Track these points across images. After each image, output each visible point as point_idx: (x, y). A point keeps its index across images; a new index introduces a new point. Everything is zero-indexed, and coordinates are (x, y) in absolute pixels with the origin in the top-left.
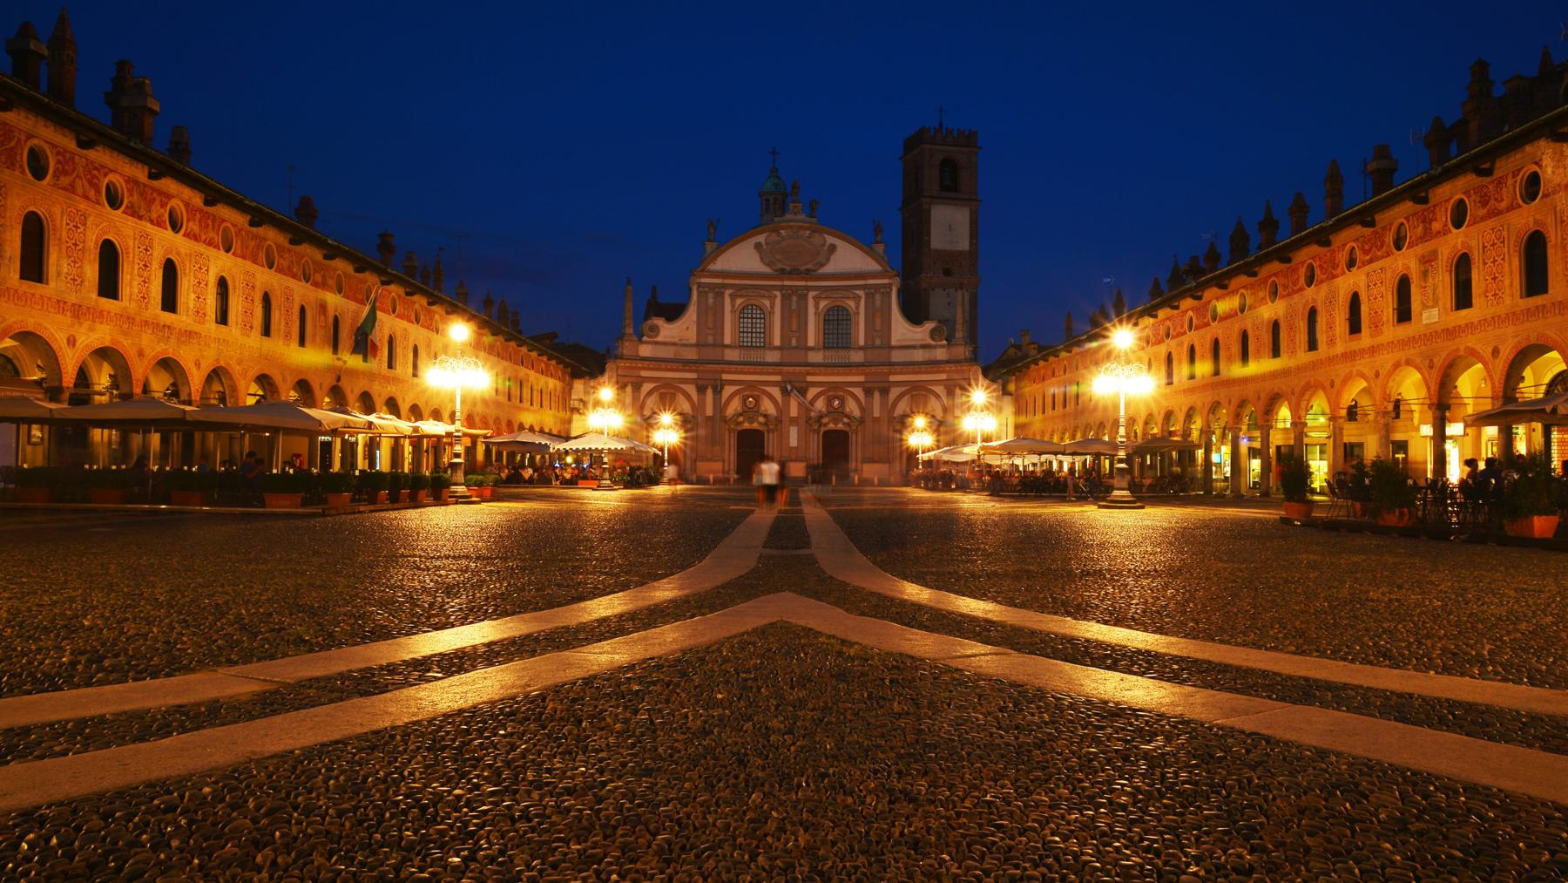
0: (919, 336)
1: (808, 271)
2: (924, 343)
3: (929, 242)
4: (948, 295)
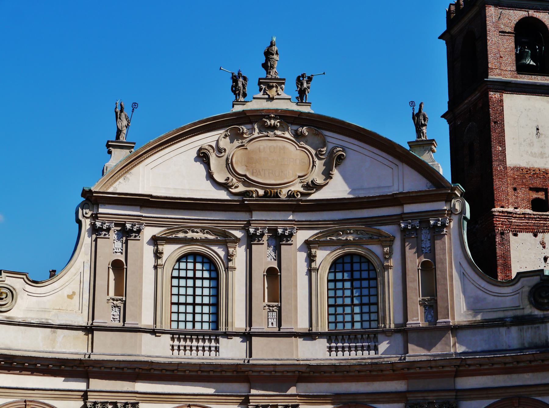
0: (508, 302)
1: (291, 195)
2: (518, 313)
3: (504, 152)
4: (543, 245)
